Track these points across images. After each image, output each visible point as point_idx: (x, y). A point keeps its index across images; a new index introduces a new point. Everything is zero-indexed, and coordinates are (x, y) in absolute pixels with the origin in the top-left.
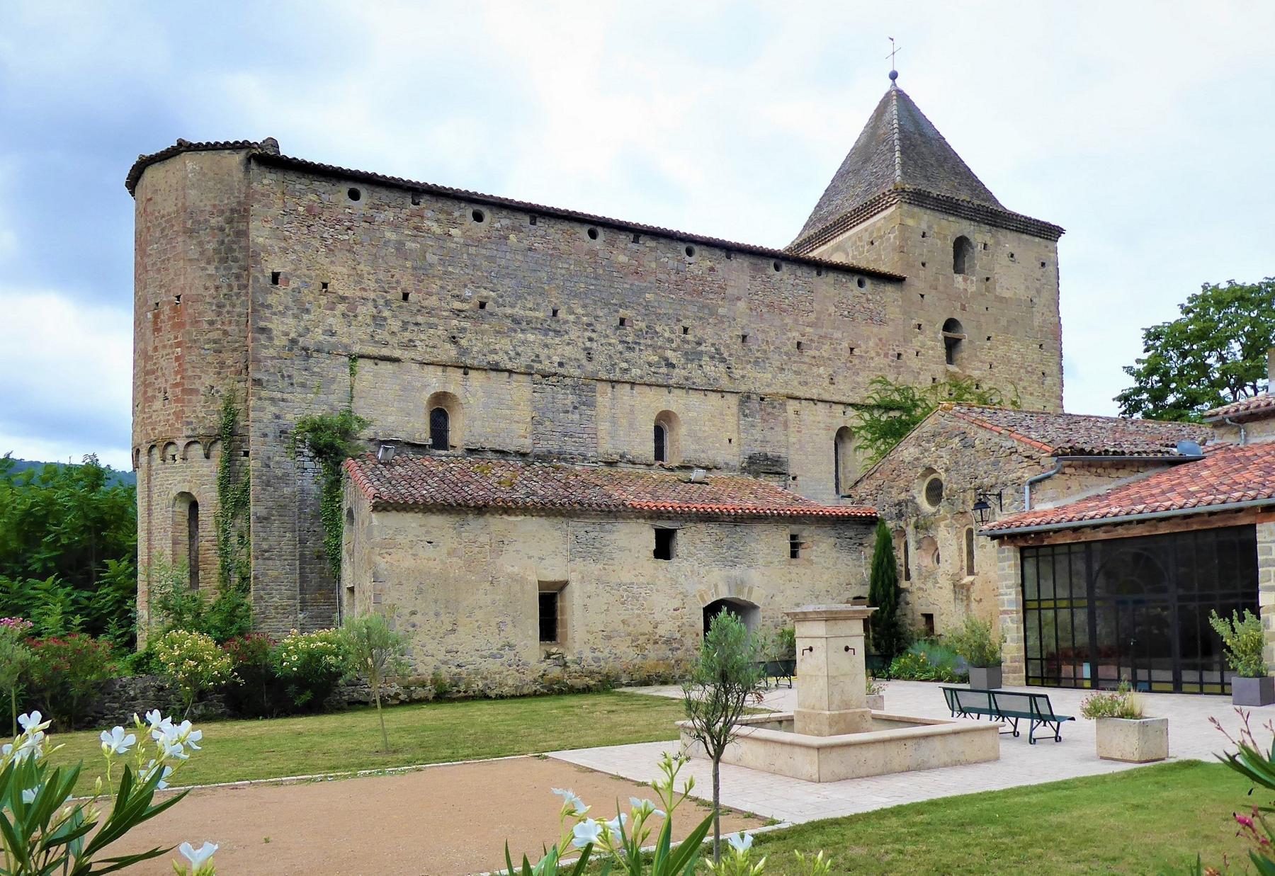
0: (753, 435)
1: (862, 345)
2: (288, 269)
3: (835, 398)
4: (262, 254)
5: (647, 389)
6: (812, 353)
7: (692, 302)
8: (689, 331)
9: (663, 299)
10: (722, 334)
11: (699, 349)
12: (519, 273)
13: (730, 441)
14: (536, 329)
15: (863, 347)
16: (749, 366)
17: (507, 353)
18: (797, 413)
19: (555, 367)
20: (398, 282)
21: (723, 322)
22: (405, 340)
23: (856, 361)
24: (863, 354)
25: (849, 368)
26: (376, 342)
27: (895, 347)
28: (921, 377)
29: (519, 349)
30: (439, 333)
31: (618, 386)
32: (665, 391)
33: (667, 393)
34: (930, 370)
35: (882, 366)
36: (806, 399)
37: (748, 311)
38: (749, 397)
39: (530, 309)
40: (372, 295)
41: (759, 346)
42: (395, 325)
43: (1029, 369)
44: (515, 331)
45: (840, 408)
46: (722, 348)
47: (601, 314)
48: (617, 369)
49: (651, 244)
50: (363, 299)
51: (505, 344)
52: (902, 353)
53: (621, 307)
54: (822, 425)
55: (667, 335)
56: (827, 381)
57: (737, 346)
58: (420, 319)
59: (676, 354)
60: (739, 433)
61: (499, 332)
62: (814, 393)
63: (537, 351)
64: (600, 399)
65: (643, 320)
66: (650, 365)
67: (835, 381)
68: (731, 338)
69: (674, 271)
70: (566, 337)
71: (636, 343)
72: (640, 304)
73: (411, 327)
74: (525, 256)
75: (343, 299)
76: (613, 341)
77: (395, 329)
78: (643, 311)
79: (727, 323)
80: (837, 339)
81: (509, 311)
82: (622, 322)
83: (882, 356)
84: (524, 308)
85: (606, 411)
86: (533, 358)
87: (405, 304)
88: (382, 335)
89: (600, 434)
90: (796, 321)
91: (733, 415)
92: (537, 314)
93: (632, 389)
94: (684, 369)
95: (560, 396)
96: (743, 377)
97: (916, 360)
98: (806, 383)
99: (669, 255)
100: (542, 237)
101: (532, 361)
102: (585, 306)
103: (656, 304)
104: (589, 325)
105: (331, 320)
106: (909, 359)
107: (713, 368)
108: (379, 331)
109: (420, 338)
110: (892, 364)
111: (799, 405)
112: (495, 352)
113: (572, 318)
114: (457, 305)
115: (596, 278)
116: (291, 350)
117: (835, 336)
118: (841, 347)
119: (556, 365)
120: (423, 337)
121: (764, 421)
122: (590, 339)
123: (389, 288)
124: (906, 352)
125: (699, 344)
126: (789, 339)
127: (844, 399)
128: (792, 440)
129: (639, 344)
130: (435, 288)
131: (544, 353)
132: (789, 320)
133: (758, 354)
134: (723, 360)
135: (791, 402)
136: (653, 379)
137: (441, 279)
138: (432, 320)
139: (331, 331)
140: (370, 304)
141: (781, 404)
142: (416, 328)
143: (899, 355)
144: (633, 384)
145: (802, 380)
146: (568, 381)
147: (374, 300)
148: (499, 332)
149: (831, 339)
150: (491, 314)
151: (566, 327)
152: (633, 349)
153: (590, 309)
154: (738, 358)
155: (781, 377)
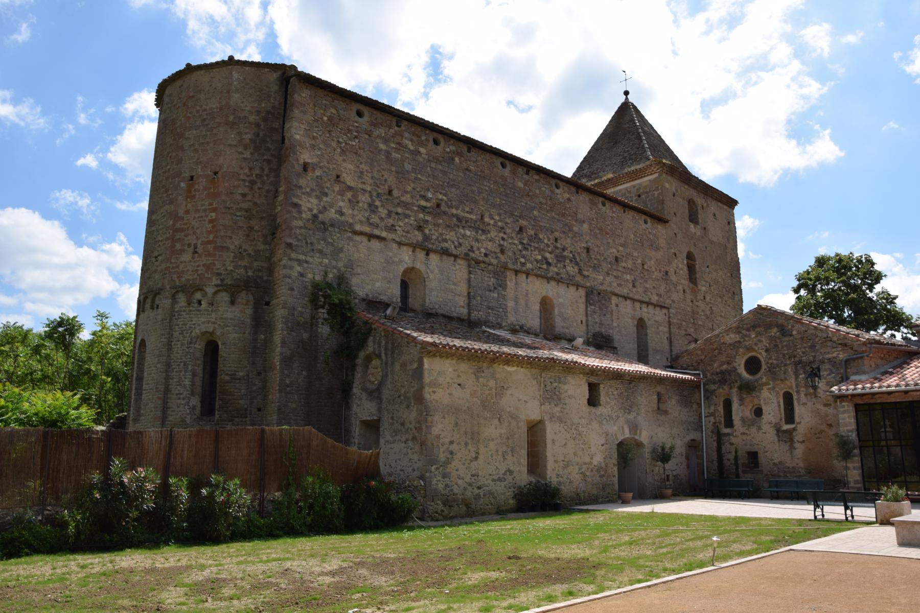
3: (637, 297)
12: (460, 185)
17: (453, 242)
22: (389, 225)
26: (371, 224)
29: (461, 241)
30: (412, 222)
31: (519, 275)
32: (545, 281)
39: (467, 212)
42: (383, 212)
44: (458, 227)
45: (638, 305)
50: (363, 189)
51: (451, 236)
55: (546, 241)
56: (631, 285)
57: (584, 255)
58: (399, 210)
61: (449, 226)
62: (625, 291)
64: (508, 283)
66: (537, 261)
70: (489, 235)
73: (393, 215)
74: (465, 174)
75: (350, 188)
76: (516, 242)
77: (383, 216)
82: (521, 229)
85: (513, 292)
88: (375, 219)
89: (508, 309)
93: (527, 278)
100: (474, 162)
101: (469, 250)
104: (502, 228)
105: (341, 204)
108: (373, 216)
112: (445, 240)
113: (492, 222)
115: (506, 196)
116: (313, 222)
119: (483, 255)
121: (601, 309)
122: (503, 239)
125: (564, 250)
127: (640, 298)
129: (530, 245)
131: (475, 245)
133: (595, 262)
134: (577, 264)
136: (539, 273)
138: (407, 212)
139: (341, 212)
140: (367, 195)
142: (396, 217)
144: (528, 274)
146: (490, 267)
147: (370, 192)
151: (488, 228)
154: (585, 263)
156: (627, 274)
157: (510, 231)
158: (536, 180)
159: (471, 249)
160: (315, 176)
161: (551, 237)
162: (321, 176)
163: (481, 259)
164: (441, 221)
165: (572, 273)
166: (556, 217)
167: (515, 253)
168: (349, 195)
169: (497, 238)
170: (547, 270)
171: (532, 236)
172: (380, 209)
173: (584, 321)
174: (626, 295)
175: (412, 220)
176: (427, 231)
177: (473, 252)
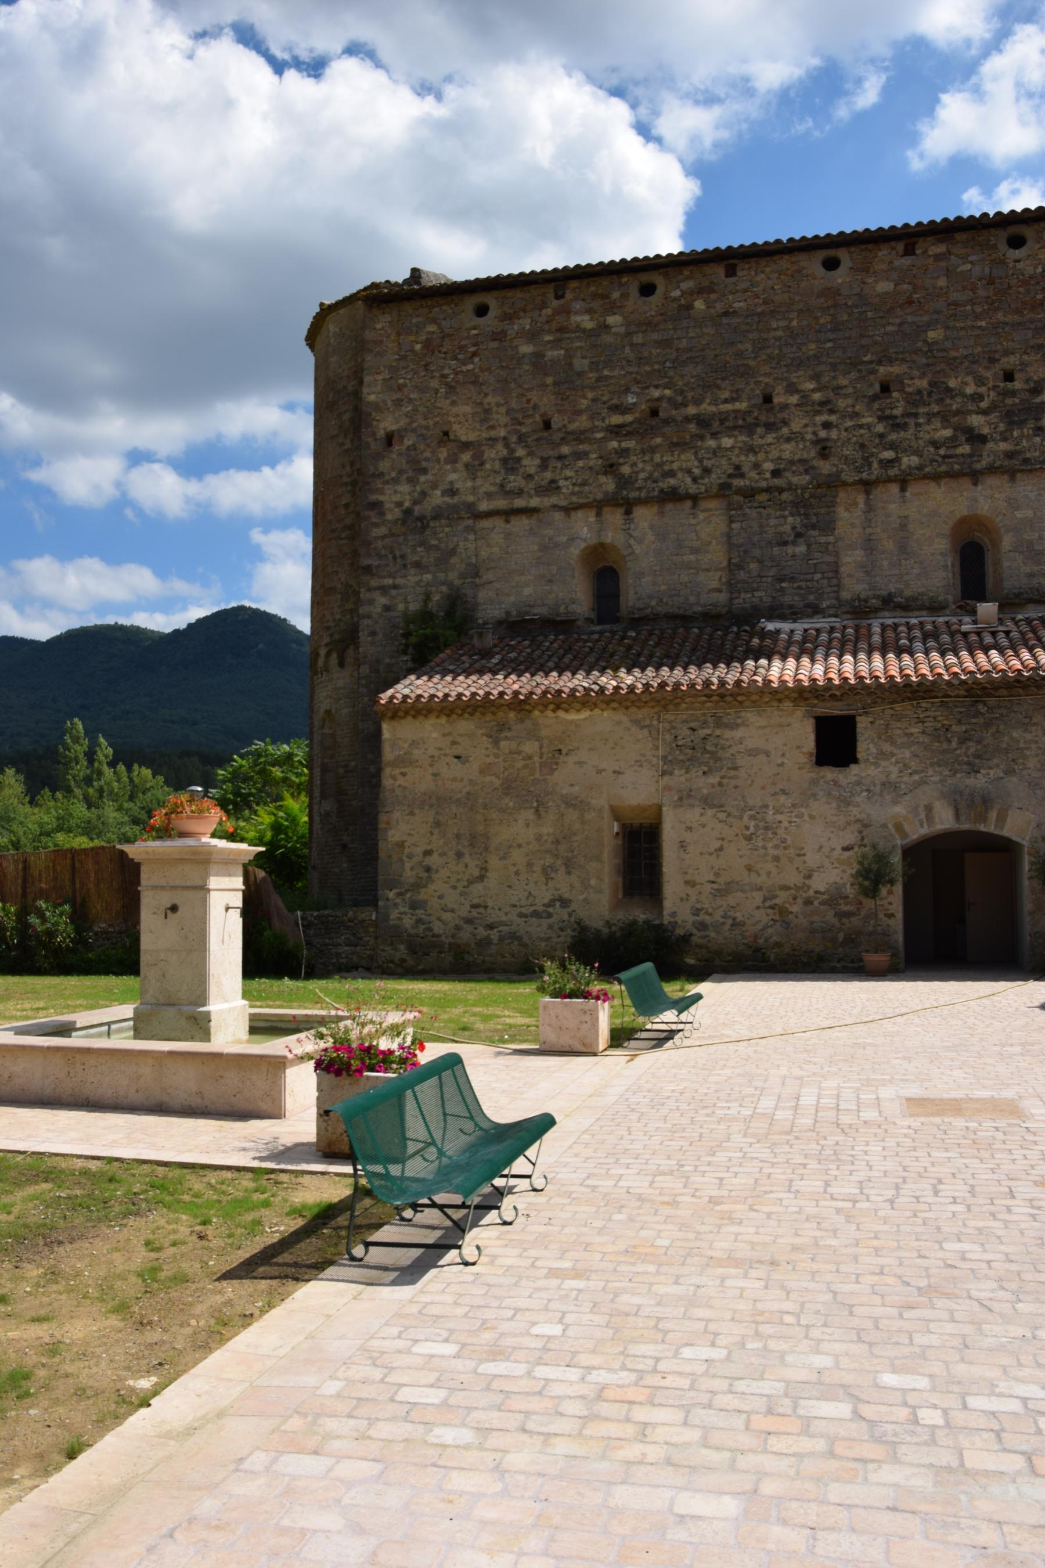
2: (402, 423)
4: (374, 414)
5: (932, 486)
9: (962, 333)
14: (735, 428)
17: (689, 471)
19: (766, 479)
20: (535, 407)
30: (592, 463)
31: (878, 492)
32: (966, 482)
33: (971, 486)
40: (502, 433)
42: (531, 464)
47: (845, 382)
48: (875, 465)
49: (941, 249)
50: (490, 439)
51: (687, 459)
53: (880, 363)
55: (969, 390)
58: (565, 450)
59: (988, 418)
61: (676, 445)
63: (734, 459)
65: (923, 375)
66: (936, 444)
70: (785, 430)
73: (553, 463)
75: (466, 446)
76: (869, 420)
78: (924, 361)
81: (692, 410)
82: (885, 388)
84: (715, 402)
86: (730, 471)
87: (546, 434)
92: (738, 406)
93: (903, 490)
94: (1005, 440)
95: (773, 522)
101: (730, 476)
102: (816, 377)
103: (948, 344)
109: (567, 478)
112: (672, 474)
114: (616, 419)
119: (768, 475)
120: (568, 473)
122: (827, 426)
123: (525, 417)
130: (584, 403)
131: (746, 461)
136: (943, 468)
137: (593, 388)
140: (500, 446)
142: (559, 465)
144: (903, 483)
146: (786, 496)
147: (505, 438)
148: (676, 445)
150: (667, 422)
152: (904, 427)
153: (825, 379)
157: (850, 401)
158: (938, 258)
159: (738, 472)
160: (404, 448)
161: (989, 374)
162: (414, 445)
163: (764, 484)
164: (659, 440)
167: (862, 446)
168: (466, 457)
169: (810, 429)
170: (971, 456)
171: (919, 392)
172: (525, 462)
175: (594, 460)
176: (626, 470)
177: (742, 476)
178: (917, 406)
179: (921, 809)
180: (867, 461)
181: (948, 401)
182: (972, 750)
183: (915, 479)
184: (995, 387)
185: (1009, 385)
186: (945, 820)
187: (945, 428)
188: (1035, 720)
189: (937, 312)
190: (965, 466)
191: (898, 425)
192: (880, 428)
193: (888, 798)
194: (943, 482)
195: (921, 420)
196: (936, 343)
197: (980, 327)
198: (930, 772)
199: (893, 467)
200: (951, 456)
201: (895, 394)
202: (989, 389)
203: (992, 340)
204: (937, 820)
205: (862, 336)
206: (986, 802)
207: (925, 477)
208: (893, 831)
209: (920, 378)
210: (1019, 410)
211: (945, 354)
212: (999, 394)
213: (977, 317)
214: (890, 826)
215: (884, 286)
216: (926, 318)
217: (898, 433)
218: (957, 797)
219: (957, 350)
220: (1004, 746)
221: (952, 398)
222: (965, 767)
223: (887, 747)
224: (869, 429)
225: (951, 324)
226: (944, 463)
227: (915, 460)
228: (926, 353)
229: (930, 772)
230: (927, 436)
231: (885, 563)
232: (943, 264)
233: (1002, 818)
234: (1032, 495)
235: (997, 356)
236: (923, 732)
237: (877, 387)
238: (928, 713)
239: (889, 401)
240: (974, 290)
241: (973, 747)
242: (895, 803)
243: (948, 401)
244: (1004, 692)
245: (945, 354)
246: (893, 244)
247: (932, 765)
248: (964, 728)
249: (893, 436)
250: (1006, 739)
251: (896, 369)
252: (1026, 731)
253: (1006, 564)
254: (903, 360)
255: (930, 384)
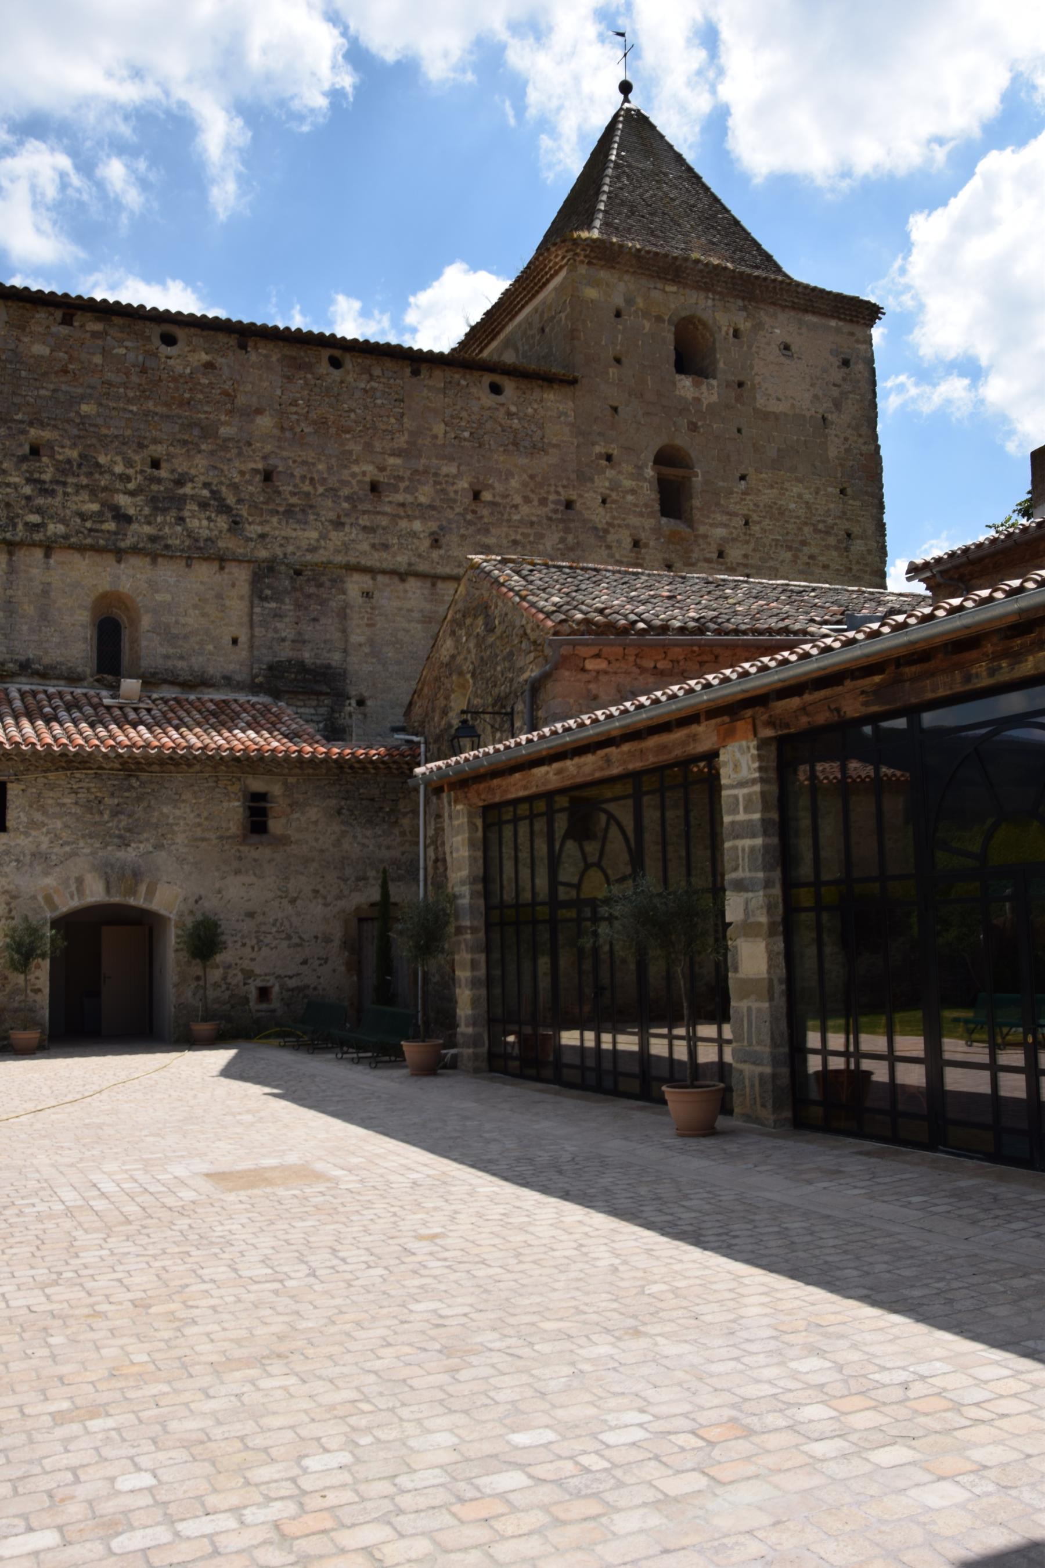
0: (276, 630)
1: (496, 485)
5: (77, 557)
6: (400, 497)
7: (168, 417)
8: (163, 465)
9: (114, 413)
10: (225, 468)
11: (181, 491)
13: (235, 641)
15: (499, 487)
16: (275, 520)
18: (367, 595)
21: (226, 449)
23: (485, 512)
24: (498, 499)
25: (470, 523)
27: (560, 489)
28: (610, 538)
32: (110, 559)
34: (627, 526)
35: (534, 519)
36: (384, 572)
37: (276, 432)
38: (271, 569)
41: (295, 486)
43: (821, 526)
46: (224, 489)
48: (20, 527)
49: (98, 327)
52: (574, 497)
53: (31, 424)
54: (416, 615)
55: (119, 469)
56: (427, 543)
57: (254, 488)
59: (134, 500)
60: (252, 627)
62: (402, 560)
65: (74, 445)
66: (83, 516)
67: (443, 541)
68: (242, 473)
69: (138, 369)
71: (58, 482)
72: (68, 421)
76: (17, 480)
78: (75, 432)
79: (234, 451)
80: (447, 475)
82: (35, 451)
83: (536, 503)
90: (368, 446)
91: (241, 598)
93: (47, 556)
94: (149, 523)
96: (263, 536)
97: (601, 510)
98: (386, 547)
99: (128, 344)
103: (100, 421)
106: (588, 508)
107: (205, 523)
110: (554, 517)
111: (371, 582)
117: (445, 470)
118: (455, 487)
124: (581, 496)
125: (180, 482)
126: (354, 475)
128: (355, 638)
129: (65, 484)
132: (356, 448)
133: (294, 500)
134: (224, 509)
135: (356, 577)
136: (89, 541)
141: (333, 581)
143: (569, 505)
144: (48, 549)
145: (377, 541)
149: (436, 475)
152: (52, 493)
155: (337, 537)
156: (410, 518)
158: (95, 335)
161: (137, 458)
165: (205, 533)
166: (160, 409)
167: (8, 505)
170: (116, 533)
171: (69, 461)
173: (243, 639)
174: (403, 568)
178: (67, 475)
179: (72, 881)
180: (12, 521)
181: (97, 476)
182: (123, 824)
183: (60, 548)
184: (142, 471)
185: (156, 472)
186: (95, 893)
187: (93, 502)
188: (184, 797)
189: (92, 387)
190: (110, 543)
191: (46, 491)
192: (27, 490)
193: (38, 869)
194: (88, 554)
195: (69, 490)
196: (88, 417)
197: (131, 412)
198: (81, 844)
199: (38, 532)
200: (97, 531)
201: (45, 459)
202: (136, 472)
203: (142, 426)
204: (88, 892)
205: (14, 393)
206: (137, 875)
207: (71, 547)
208: (42, 903)
209: (70, 448)
210: (164, 498)
211: (97, 430)
212: (145, 478)
213: (129, 401)
214: (40, 898)
215: (40, 349)
216: (80, 391)
217: (46, 498)
218: (108, 870)
219: (109, 428)
220: (154, 820)
221: (101, 473)
222: (116, 840)
223: (38, 816)
224: (16, 489)
225: (104, 402)
226: (89, 536)
227: (61, 529)
228: (79, 424)
229: (81, 844)
230: (74, 507)
231: (25, 628)
232: (100, 342)
233: (151, 892)
234: (172, 581)
235: (146, 443)
236: (76, 803)
237: (27, 449)
238: (82, 784)
239: (38, 464)
240: (127, 374)
241: (124, 821)
242: (46, 874)
243: (97, 476)
244: (156, 768)
245: (97, 430)
246: (52, 309)
247: (83, 836)
248: (116, 801)
249: (40, 501)
250: (156, 814)
251: (47, 434)
252: (175, 807)
253: (144, 643)
254: (55, 427)
255: (80, 456)
